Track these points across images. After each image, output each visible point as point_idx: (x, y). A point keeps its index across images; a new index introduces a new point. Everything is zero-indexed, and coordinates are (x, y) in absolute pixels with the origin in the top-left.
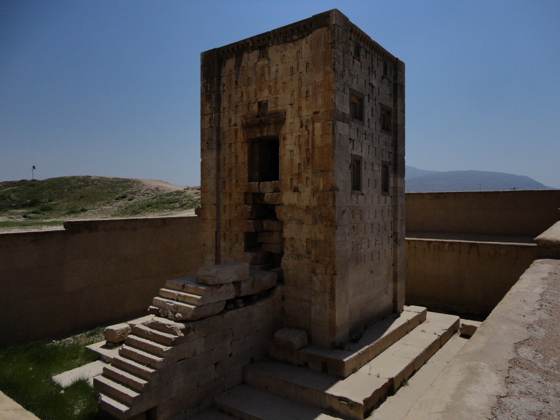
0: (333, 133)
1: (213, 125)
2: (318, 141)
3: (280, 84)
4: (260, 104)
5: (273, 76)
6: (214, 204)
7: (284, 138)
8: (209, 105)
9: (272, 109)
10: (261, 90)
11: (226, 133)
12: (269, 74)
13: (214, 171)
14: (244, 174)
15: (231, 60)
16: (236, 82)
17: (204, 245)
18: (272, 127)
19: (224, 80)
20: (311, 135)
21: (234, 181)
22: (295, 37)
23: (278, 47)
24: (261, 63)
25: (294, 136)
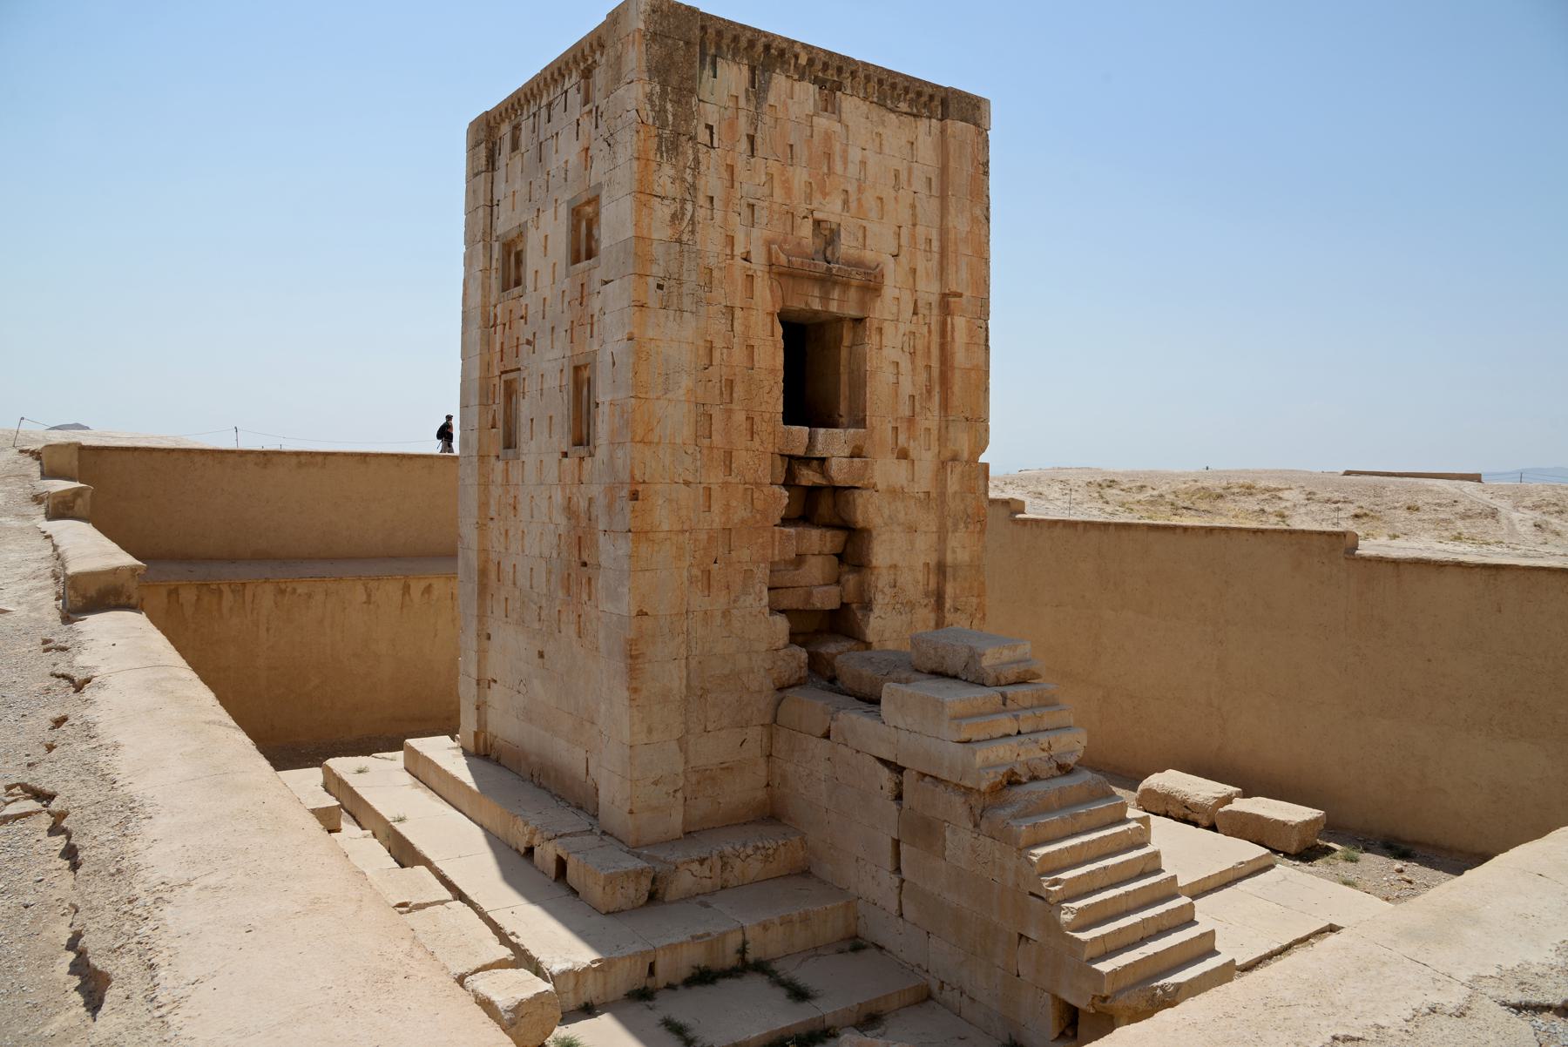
0: (987, 347)
1: (685, 238)
2: (960, 357)
4: (817, 223)
5: (853, 170)
6: (687, 483)
7: (880, 330)
8: (668, 170)
9: (851, 251)
10: (825, 195)
11: (715, 274)
12: (845, 163)
13: (686, 382)
15: (735, 68)
16: (751, 139)
17: (641, 613)
18: (853, 294)
19: (711, 114)
20: (936, 338)
21: (740, 417)
22: (903, 106)
23: (864, 107)
24: (823, 122)
25: (901, 331)
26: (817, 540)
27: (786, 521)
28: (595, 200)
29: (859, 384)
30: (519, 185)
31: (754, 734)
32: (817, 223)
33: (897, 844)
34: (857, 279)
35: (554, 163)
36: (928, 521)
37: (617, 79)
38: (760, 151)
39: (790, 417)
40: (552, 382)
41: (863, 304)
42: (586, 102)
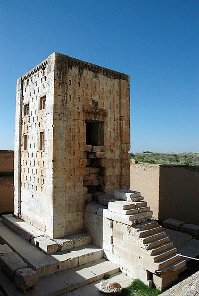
3: (105, 95)
4: (93, 101)
5: (101, 90)
6: (65, 158)
8: (61, 90)
12: (99, 88)
13: (65, 136)
14: (84, 140)
16: (79, 83)
17: (55, 187)
19: (70, 78)
20: (119, 126)
23: (103, 76)
24: (94, 80)
26: (94, 170)
27: (87, 166)
28: (45, 97)
29: (103, 136)
30: (28, 92)
31: (80, 214)
32: (93, 101)
33: (112, 237)
34: (102, 113)
35: (36, 88)
36: (118, 165)
37: (49, 71)
38: (81, 86)
39: (88, 143)
40: (35, 135)
41: (103, 119)
42: (44, 75)
